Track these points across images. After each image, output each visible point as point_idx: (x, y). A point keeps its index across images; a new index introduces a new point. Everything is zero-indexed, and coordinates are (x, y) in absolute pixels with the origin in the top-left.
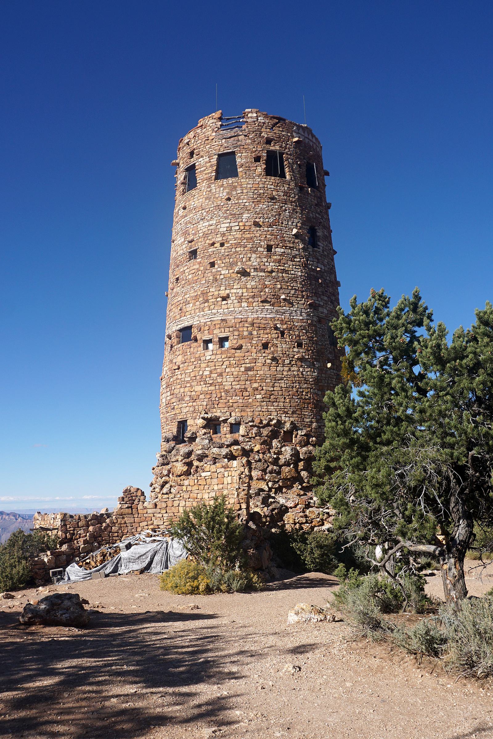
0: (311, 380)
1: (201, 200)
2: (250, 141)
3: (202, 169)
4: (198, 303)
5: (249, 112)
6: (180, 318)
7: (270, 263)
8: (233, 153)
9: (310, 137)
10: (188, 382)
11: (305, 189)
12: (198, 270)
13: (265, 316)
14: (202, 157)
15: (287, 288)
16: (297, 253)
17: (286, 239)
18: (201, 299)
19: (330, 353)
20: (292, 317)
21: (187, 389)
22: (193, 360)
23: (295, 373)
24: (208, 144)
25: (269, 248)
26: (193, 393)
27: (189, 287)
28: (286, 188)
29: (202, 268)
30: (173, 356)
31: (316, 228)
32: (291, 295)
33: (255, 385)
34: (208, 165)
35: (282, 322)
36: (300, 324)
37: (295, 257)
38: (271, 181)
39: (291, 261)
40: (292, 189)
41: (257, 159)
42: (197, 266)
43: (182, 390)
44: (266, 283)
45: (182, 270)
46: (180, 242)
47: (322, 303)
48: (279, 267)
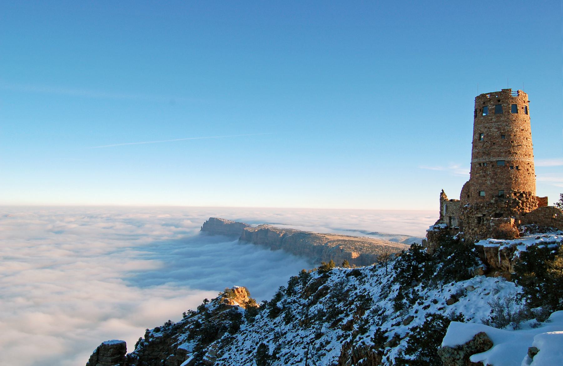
1: (505, 119)
3: (505, 108)
4: (507, 154)
6: (498, 157)
8: (516, 105)
10: (505, 179)
12: (506, 143)
14: (505, 103)
18: (508, 153)
21: (504, 181)
22: (506, 172)
24: (507, 99)
26: (507, 183)
27: (502, 148)
29: (508, 142)
30: (494, 169)
33: (526, 182)
34: (508, 107)
41: (523, 108)
42: (506, 141)
43: (501, 181)
45: (497, 141)
46: (495, 131)
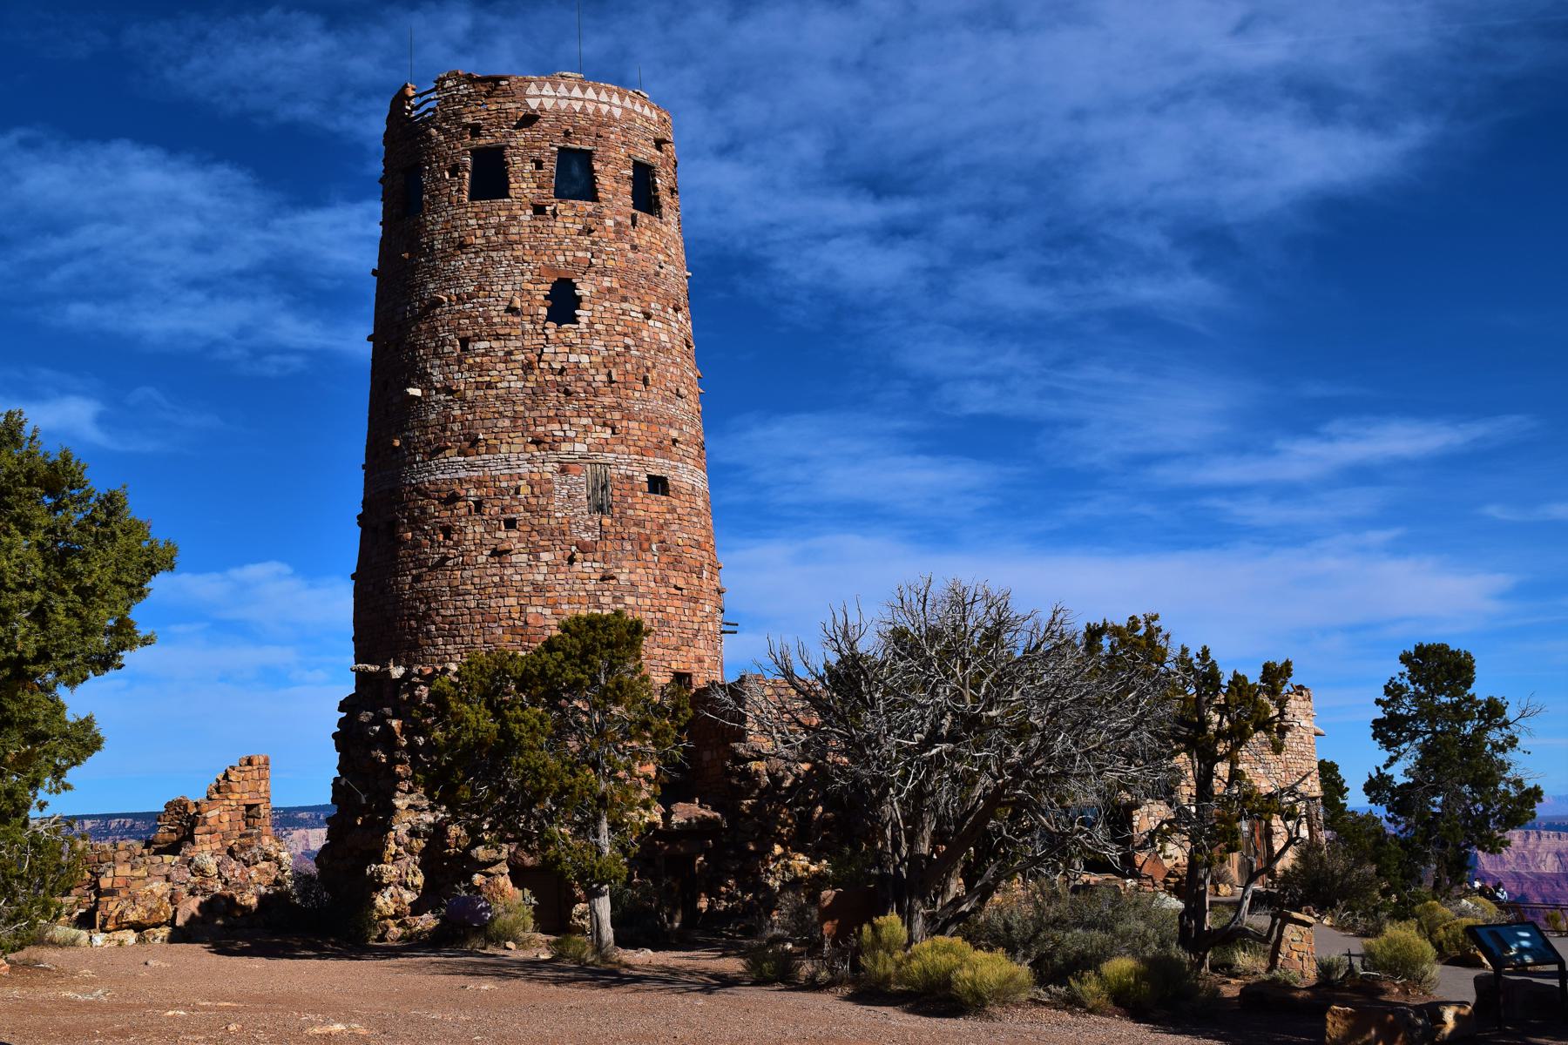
0: (525, 589)
2: (442, 138)
5: (444, 80)
7: (462, 373)
9: (577, 92)
11: (548, 208)
13: (448, 476)
15: (489, 415)
16: (519, 344)
17: (495, 320)
19: (587, 529)
20: (498, 473)
23: (496, 579)
25: (465, 342)
28: (503, 219)
31: (574, 281)
32: (496, 430)
35: (479, 484)
36: (513, 483)
37: (510, 353)
38: (476, 210)
39: (506, 362)
40: (515, 218)
44: (455, 413)
47: (571, 434)
48: (480, 379)
